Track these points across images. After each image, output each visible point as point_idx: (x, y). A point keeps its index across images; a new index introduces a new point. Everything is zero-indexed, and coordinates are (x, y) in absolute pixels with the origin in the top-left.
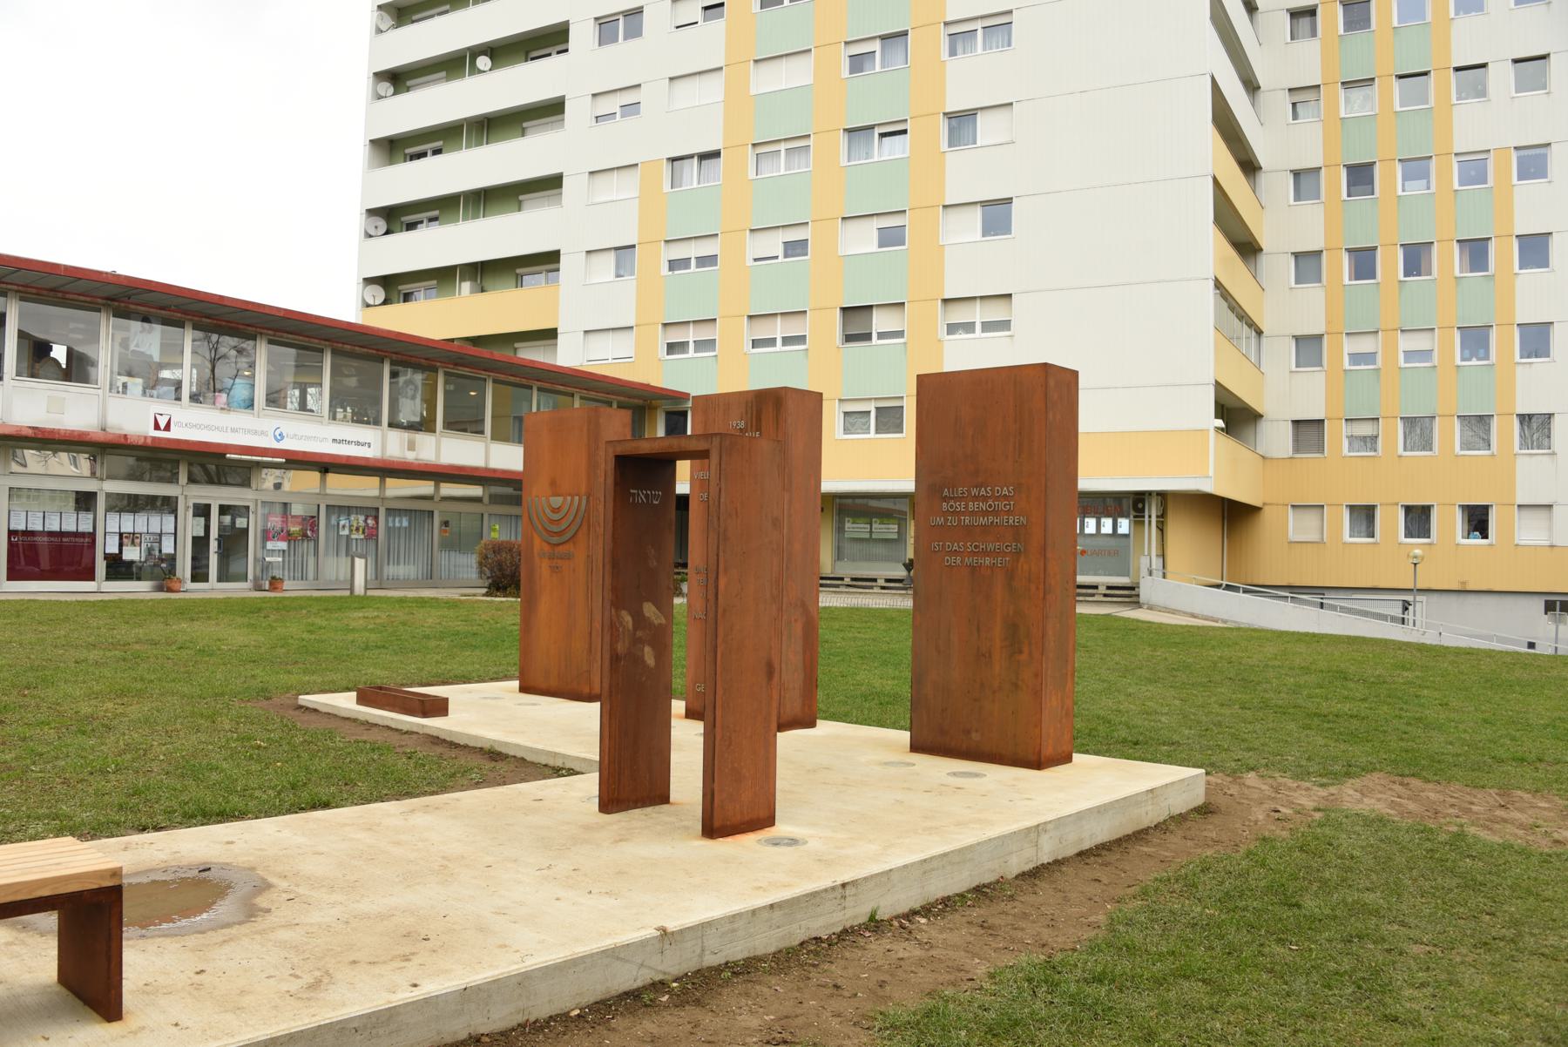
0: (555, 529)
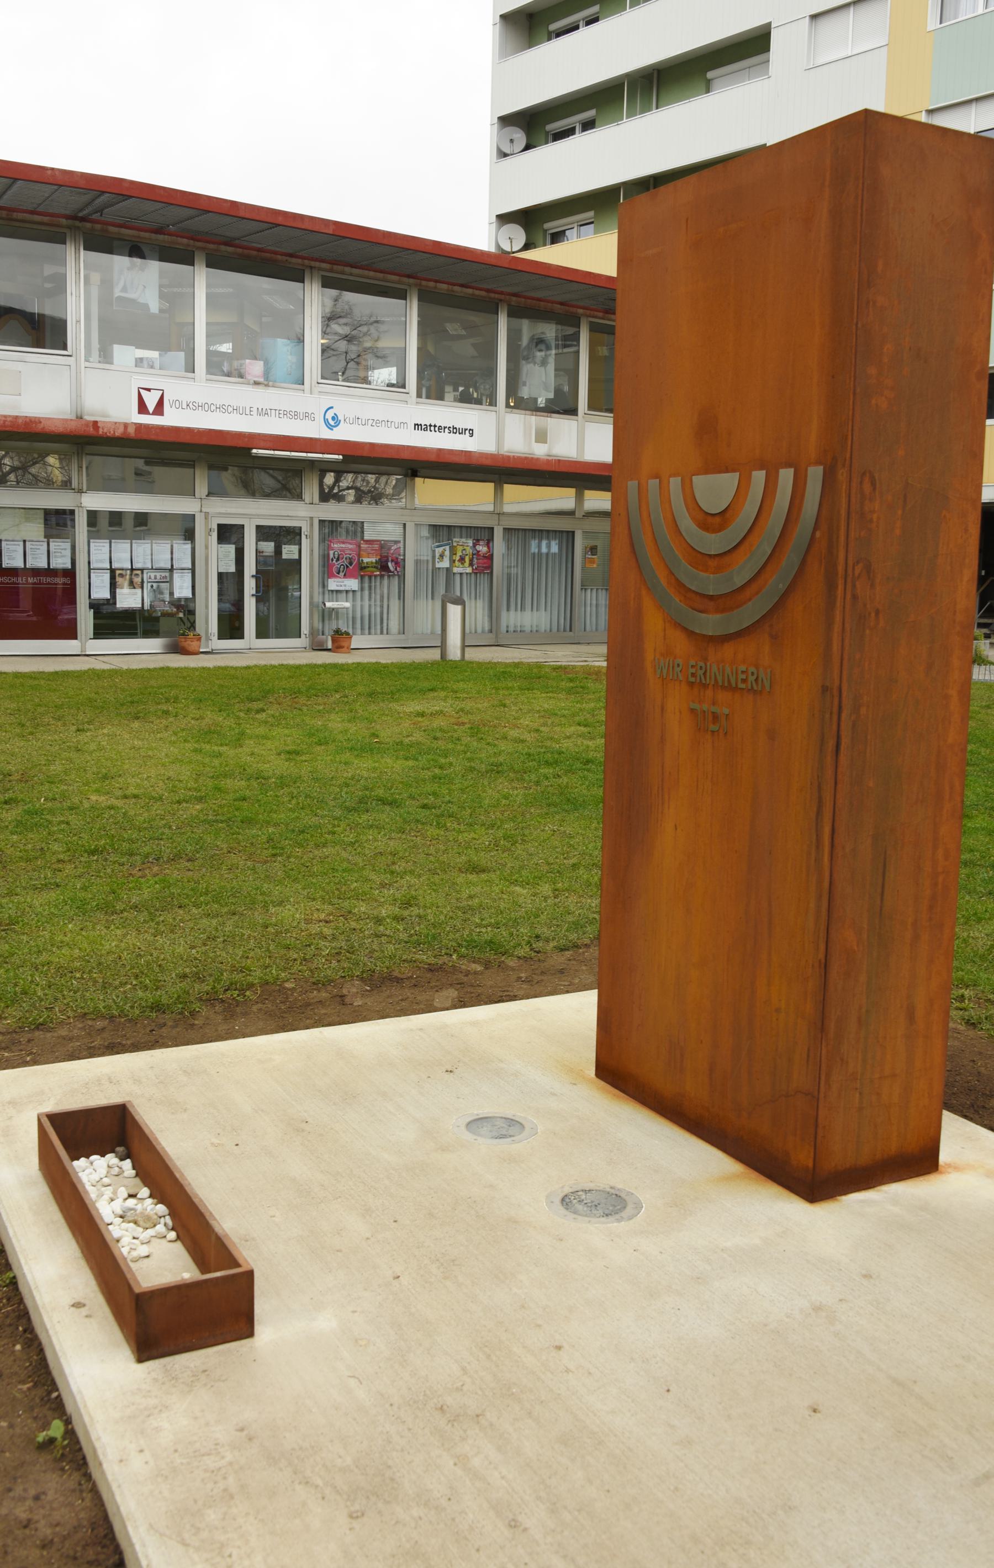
0: (711, 583)
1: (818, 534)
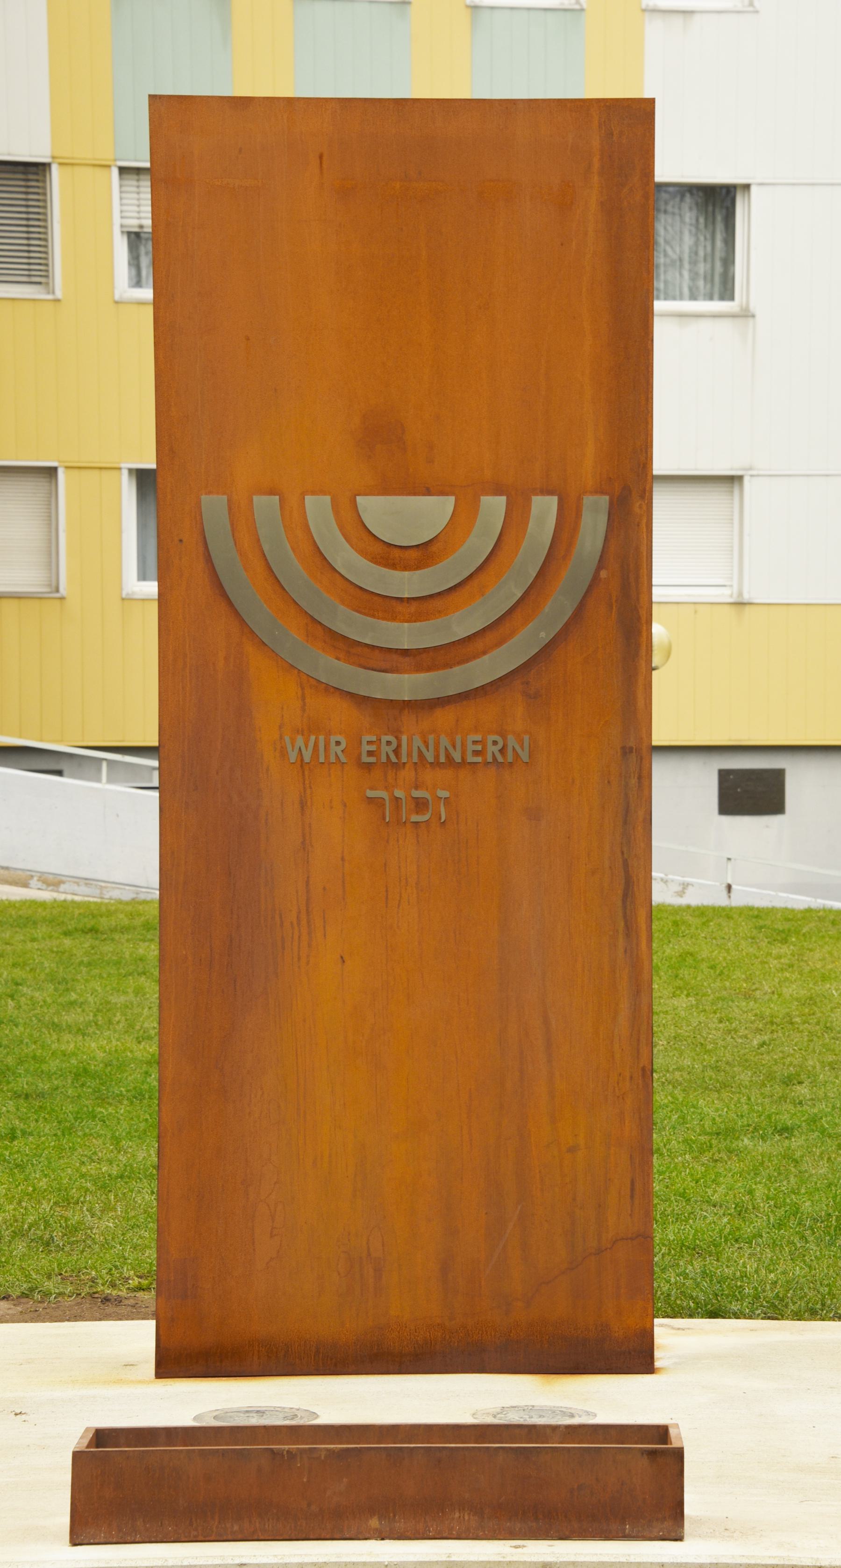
1: (603, 574)
